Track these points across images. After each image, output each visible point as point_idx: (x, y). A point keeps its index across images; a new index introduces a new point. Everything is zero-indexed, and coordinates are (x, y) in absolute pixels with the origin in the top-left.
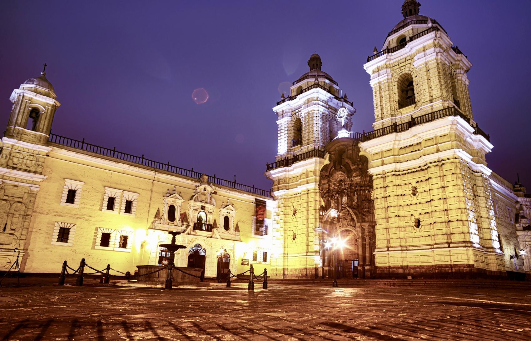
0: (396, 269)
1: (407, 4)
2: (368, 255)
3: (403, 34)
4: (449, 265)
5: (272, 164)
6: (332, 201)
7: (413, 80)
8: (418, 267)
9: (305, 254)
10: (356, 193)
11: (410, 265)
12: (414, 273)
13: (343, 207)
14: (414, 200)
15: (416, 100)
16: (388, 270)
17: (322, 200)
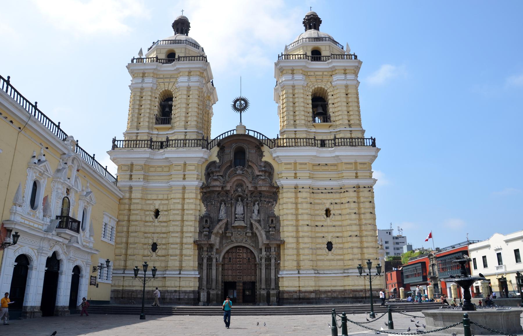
0: (307, 294)
1: (312, 16)
2: (273, 276)
3: (320, 46)
4: (363, 289)
5: (120, 141)
6: (222, 208)
7: (330, 97)
8: (329, 292)
9: (178, 273)
10: (256, 203)
11: (321, 289)
12: (325, 297)
13: (236, 218)
14: (329, 221)
15: (332, 119)
16: (298, 294)
17: (202, 205)
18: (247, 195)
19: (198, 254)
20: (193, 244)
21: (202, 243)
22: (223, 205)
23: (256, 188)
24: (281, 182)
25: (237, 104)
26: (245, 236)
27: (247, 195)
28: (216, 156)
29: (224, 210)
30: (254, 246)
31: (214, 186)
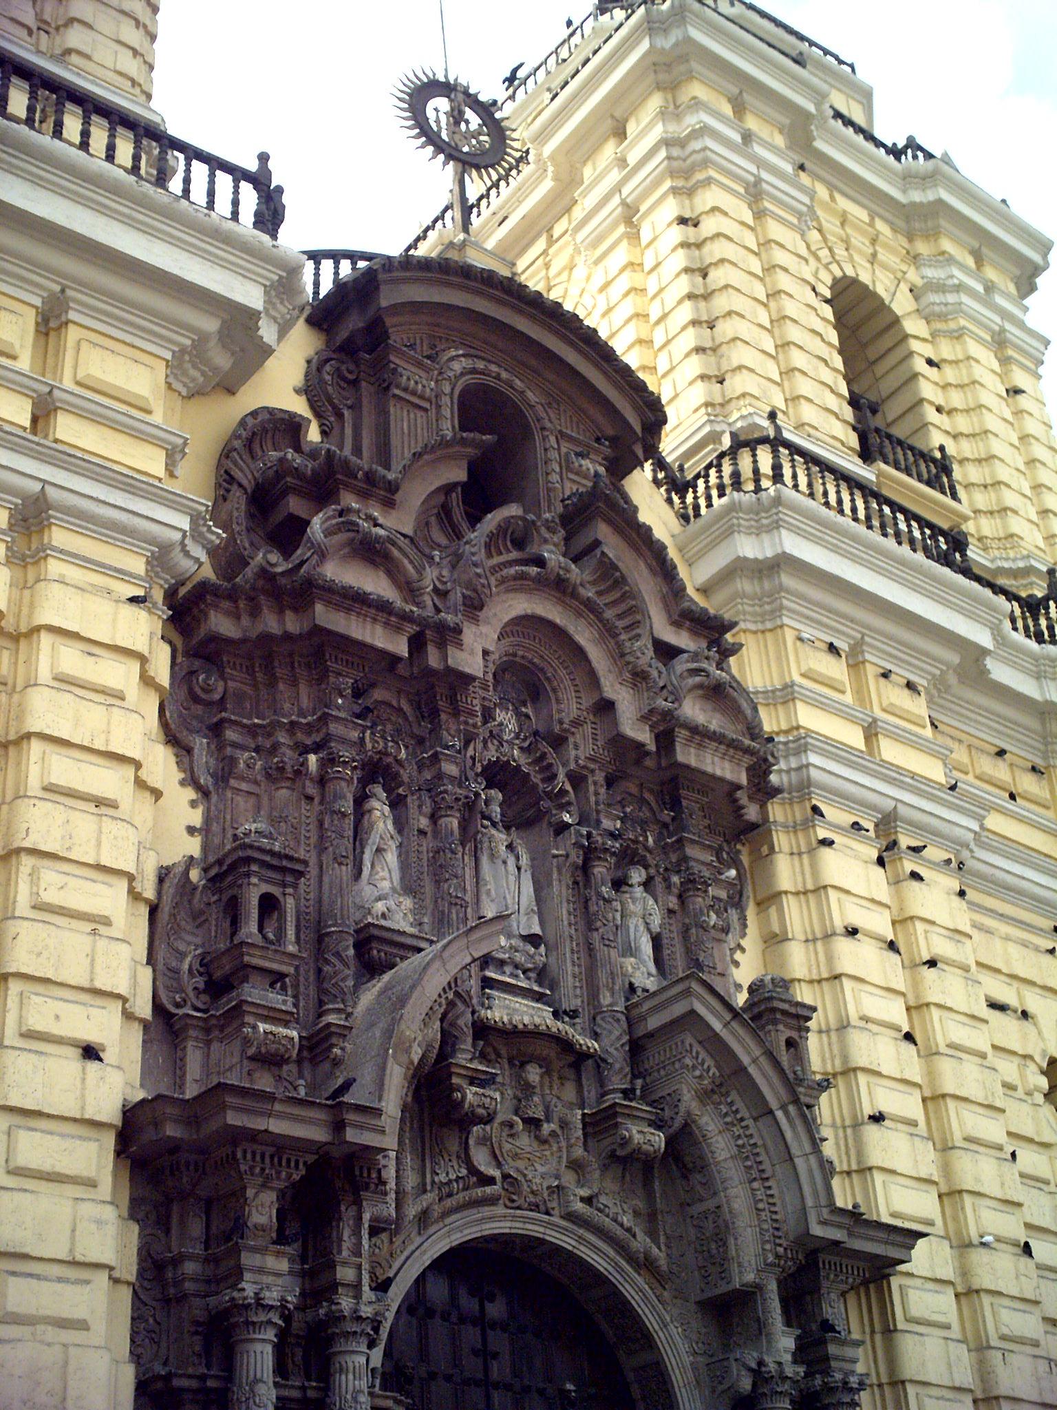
18: (577, 780)
19: (141, 1273)
20: (110, 1140)
21: (278, 1126)
22: (380, 810)
23: (665, 739)
24: (814, 758)
25: (430, 113)
26: (579, 1152)
27: (577, 780)
28: (298, 391)
29: (391, 857)
30: (663, 1263)
31: (355, 601)
